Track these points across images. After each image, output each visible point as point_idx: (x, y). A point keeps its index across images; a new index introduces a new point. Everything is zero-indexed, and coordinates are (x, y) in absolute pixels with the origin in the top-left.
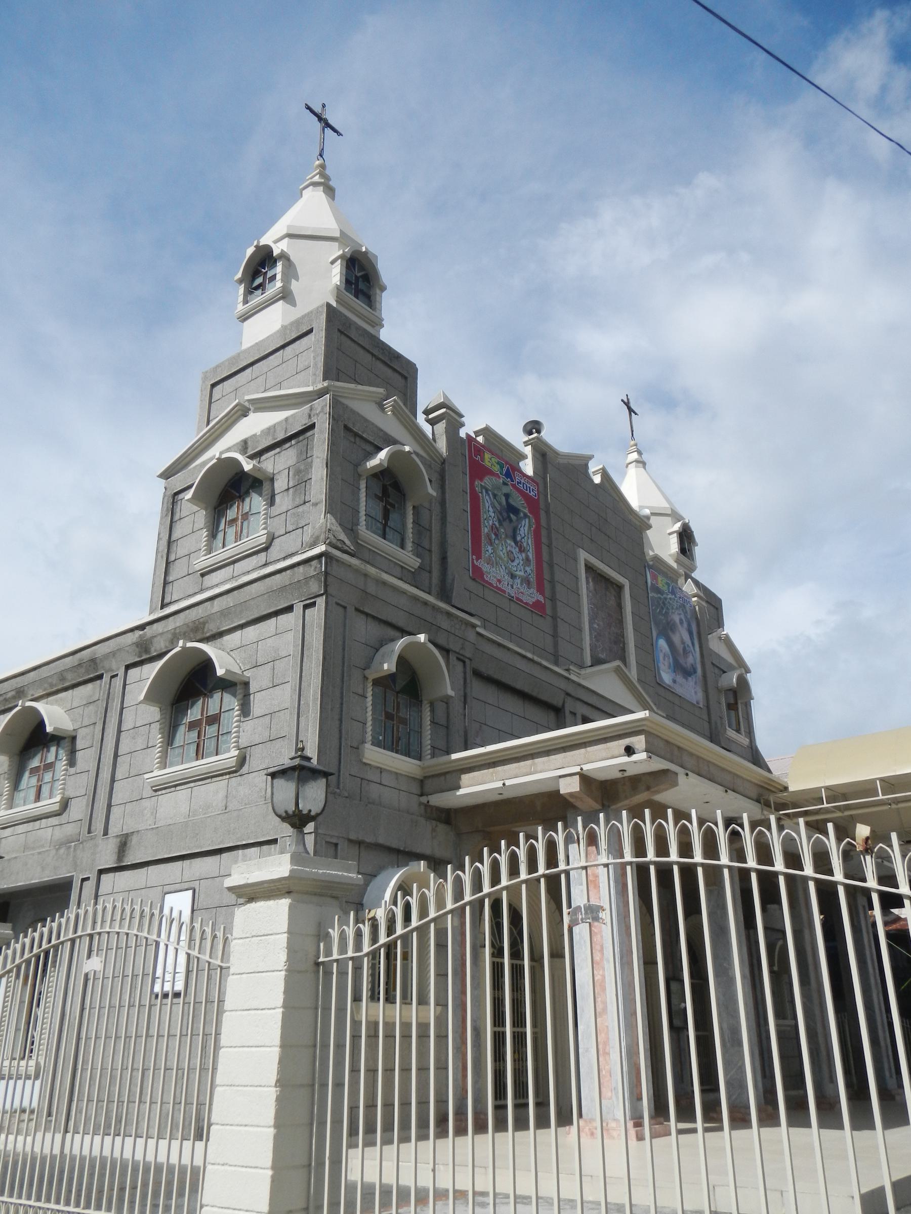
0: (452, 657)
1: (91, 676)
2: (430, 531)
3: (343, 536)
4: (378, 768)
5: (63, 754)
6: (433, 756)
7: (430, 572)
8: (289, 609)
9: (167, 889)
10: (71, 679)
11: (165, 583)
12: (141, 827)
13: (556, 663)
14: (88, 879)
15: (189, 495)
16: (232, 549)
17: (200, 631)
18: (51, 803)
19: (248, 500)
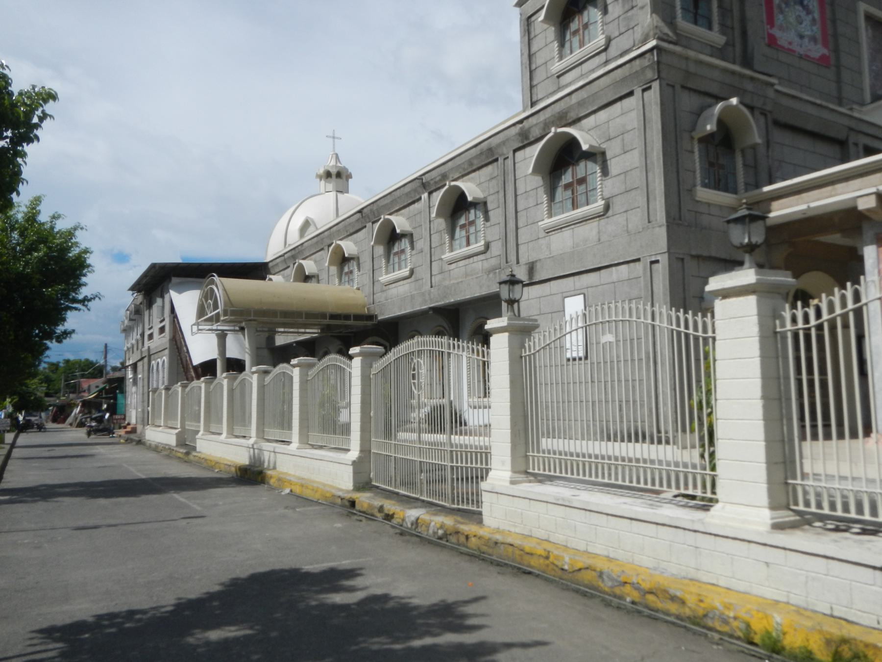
0: (757, 113)
2: (731, 11)
3: (666, 30)
4: (706, 203)
5: (480, 215)
6: (746, 190)
7: (734, 46)
8: (631, 94)
9: (565, 295)
11: (532, 87)
12: (542, 257)
13: (840, 104)
15: (542, 15)
16: (578, 54)
17: (563, 119)
18: (479, 246)
19: (586, 13)
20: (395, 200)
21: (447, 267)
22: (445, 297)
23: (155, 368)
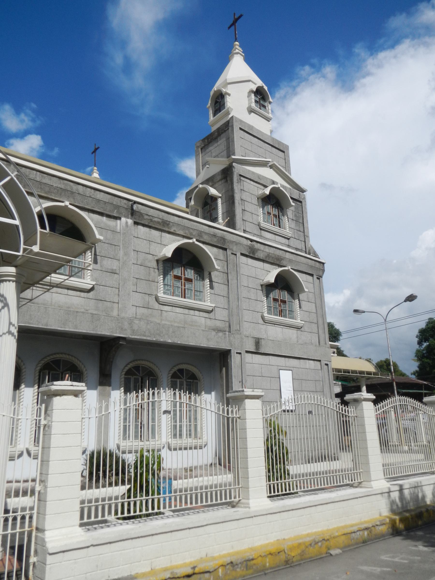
1: (219, 245)
8: (312, 275)
10: (206, 238)
14: (240, 353)
20: (72, 193)
21: (156, 306)
22: (159, 335)
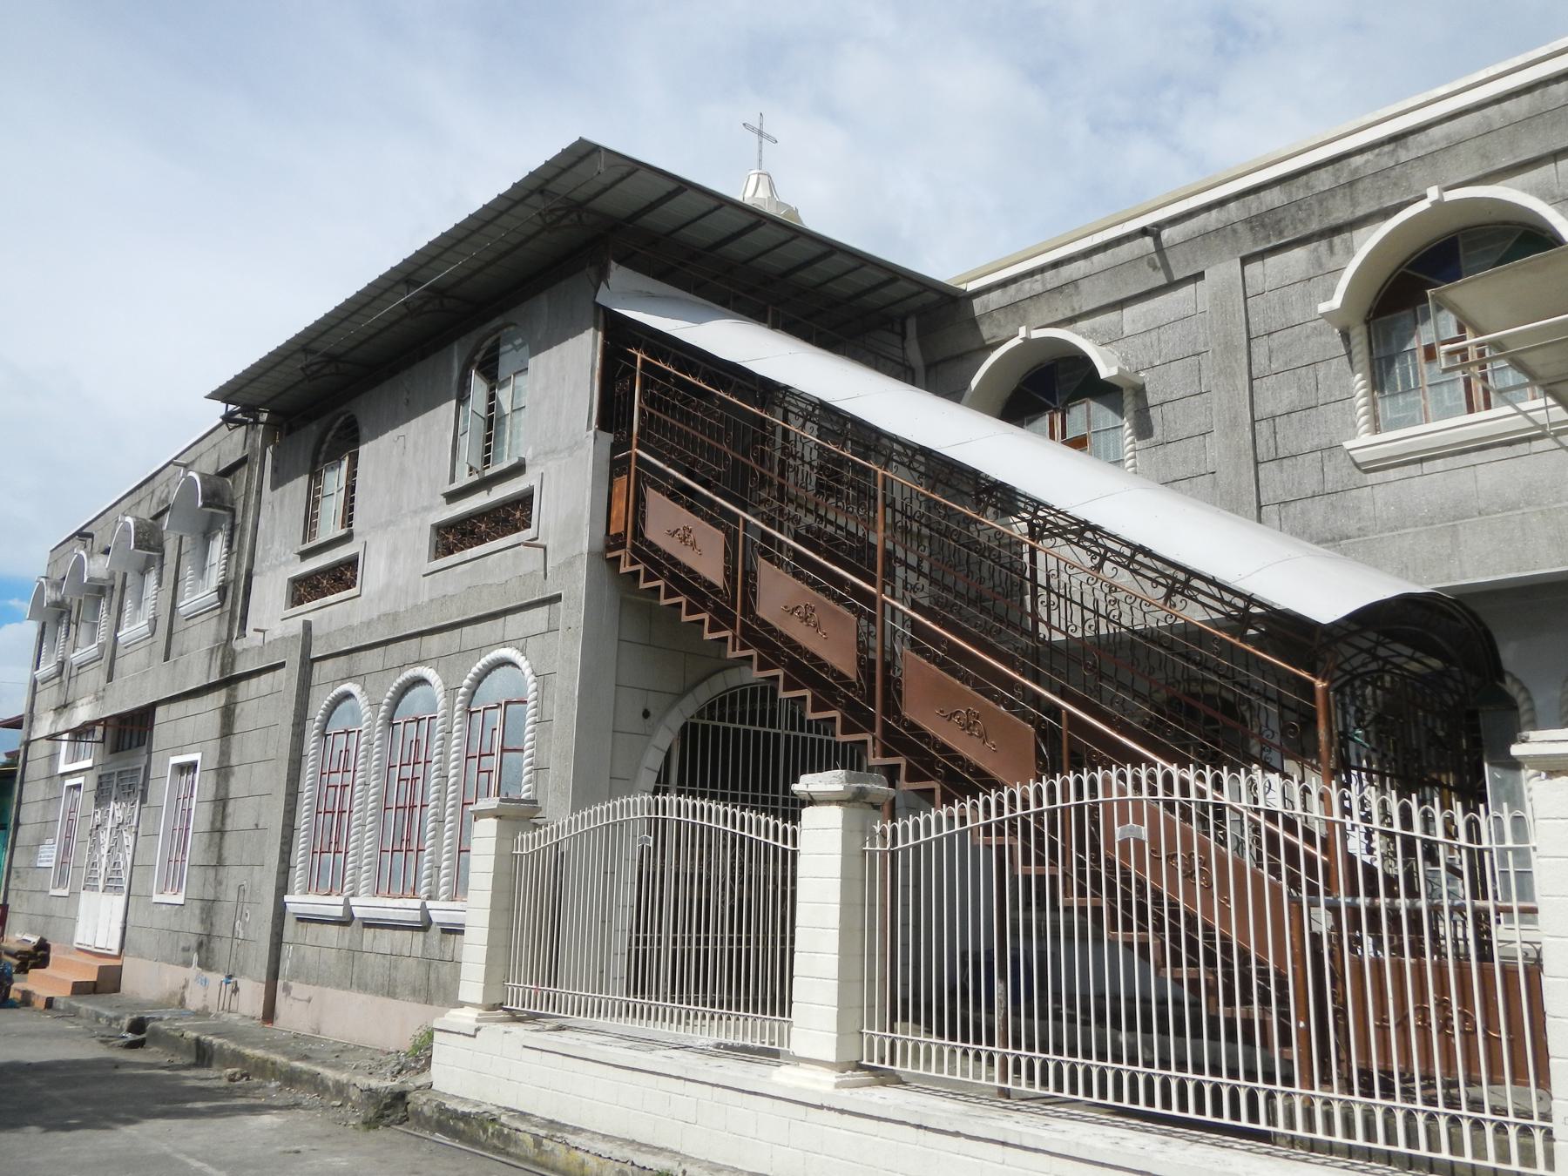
23: (365, 711)
